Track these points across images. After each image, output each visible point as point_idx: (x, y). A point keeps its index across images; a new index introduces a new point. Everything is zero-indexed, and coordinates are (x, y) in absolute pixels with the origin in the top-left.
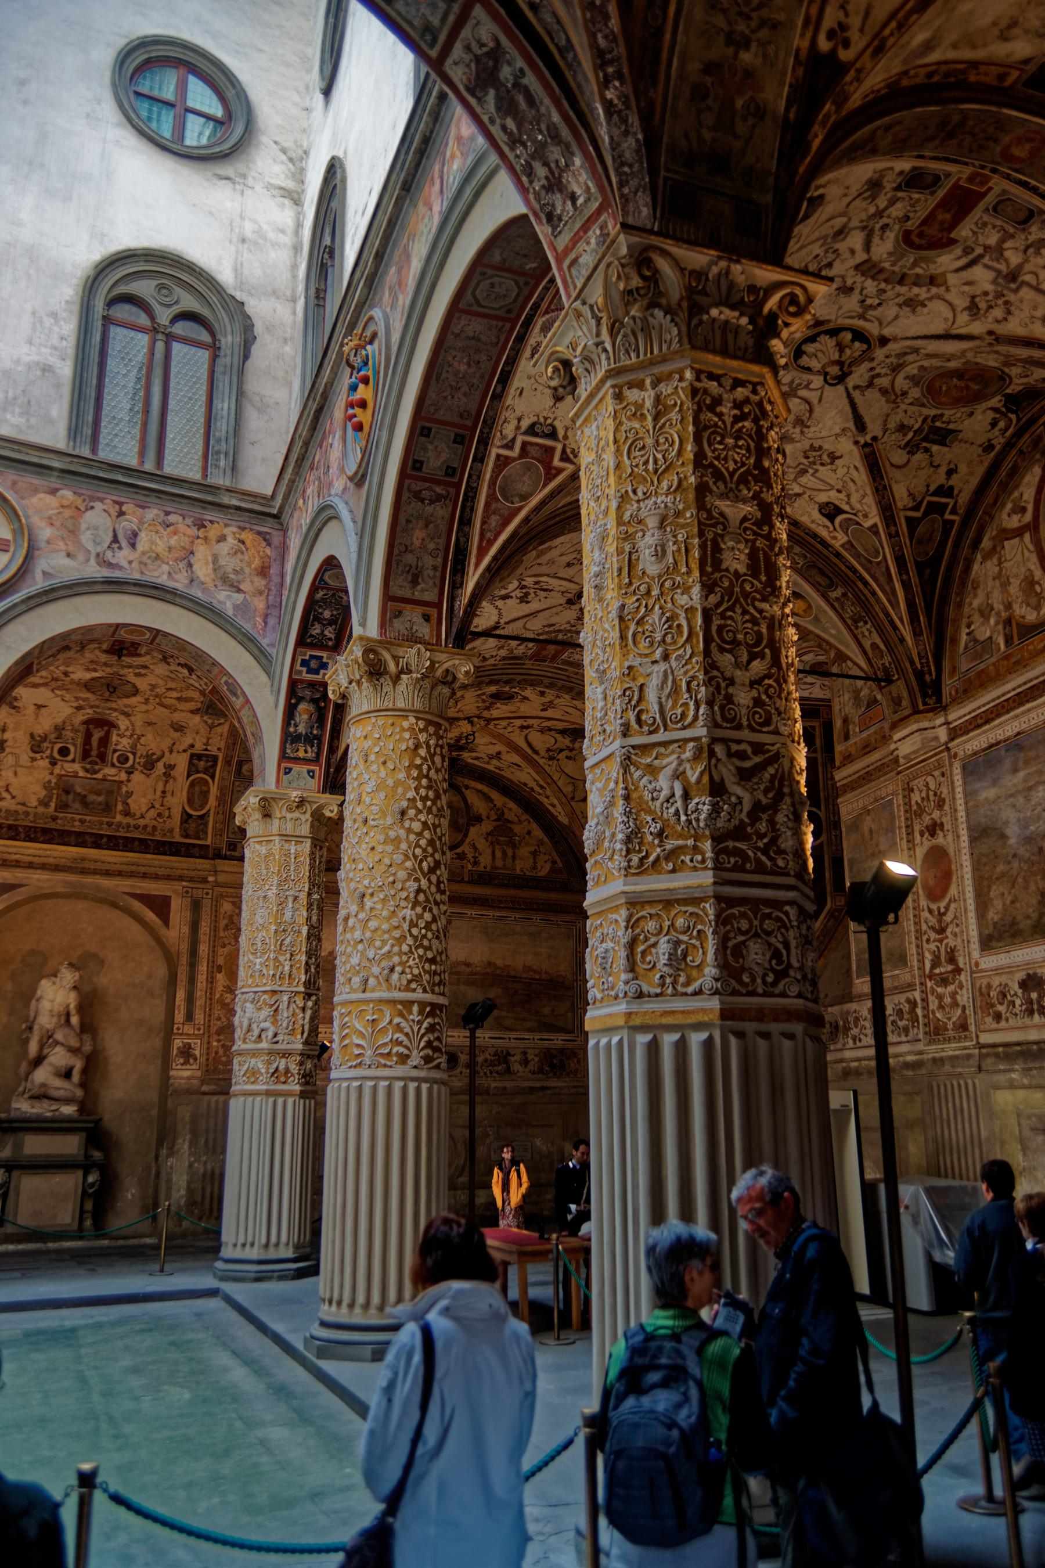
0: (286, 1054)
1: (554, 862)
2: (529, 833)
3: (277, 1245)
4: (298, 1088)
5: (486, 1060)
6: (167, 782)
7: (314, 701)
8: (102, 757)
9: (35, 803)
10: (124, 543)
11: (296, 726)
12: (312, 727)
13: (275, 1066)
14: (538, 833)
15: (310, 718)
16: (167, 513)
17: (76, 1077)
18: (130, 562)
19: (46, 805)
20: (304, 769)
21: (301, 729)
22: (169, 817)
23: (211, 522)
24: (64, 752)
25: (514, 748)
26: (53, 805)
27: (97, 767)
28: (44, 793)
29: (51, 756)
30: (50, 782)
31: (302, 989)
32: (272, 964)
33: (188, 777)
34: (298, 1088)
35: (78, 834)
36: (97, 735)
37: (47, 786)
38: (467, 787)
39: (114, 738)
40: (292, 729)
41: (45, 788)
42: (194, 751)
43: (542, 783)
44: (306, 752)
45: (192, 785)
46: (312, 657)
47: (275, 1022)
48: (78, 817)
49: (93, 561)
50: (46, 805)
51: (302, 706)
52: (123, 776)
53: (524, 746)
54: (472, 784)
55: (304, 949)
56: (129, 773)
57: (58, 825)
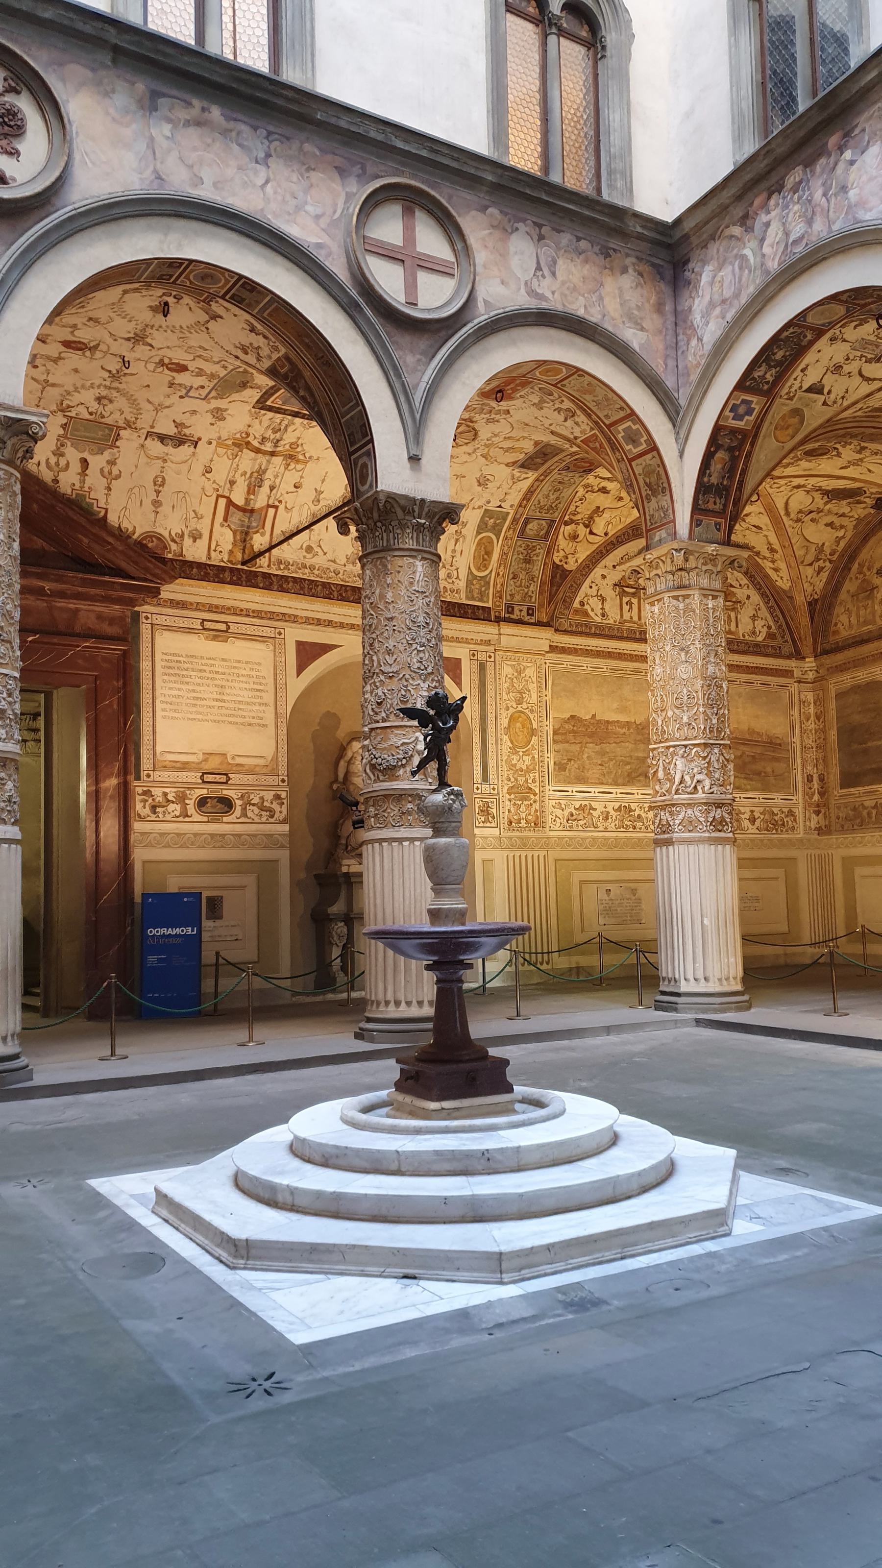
1: (769, 627)
2: (748, 597)
6: (457, 540)
7: (730, 449)
10: (546, 271)
12: (723, 478)
13: (712, 815)
14: (756, 598)
15: (723, 468)
16: (579, 239)
18: (553, 293)
21: (714, 480)
22: (457, 578)
23: (614, 250)
32: (702, 716)
33: (478, 533)
40: (706, 479)
42: (490, 507)
43: (777, 546)
44: (715, 503)
45: (479, 544)
46: (743, 401)
47: (709, 775)
49: (523, 291)
51: (720, 455)
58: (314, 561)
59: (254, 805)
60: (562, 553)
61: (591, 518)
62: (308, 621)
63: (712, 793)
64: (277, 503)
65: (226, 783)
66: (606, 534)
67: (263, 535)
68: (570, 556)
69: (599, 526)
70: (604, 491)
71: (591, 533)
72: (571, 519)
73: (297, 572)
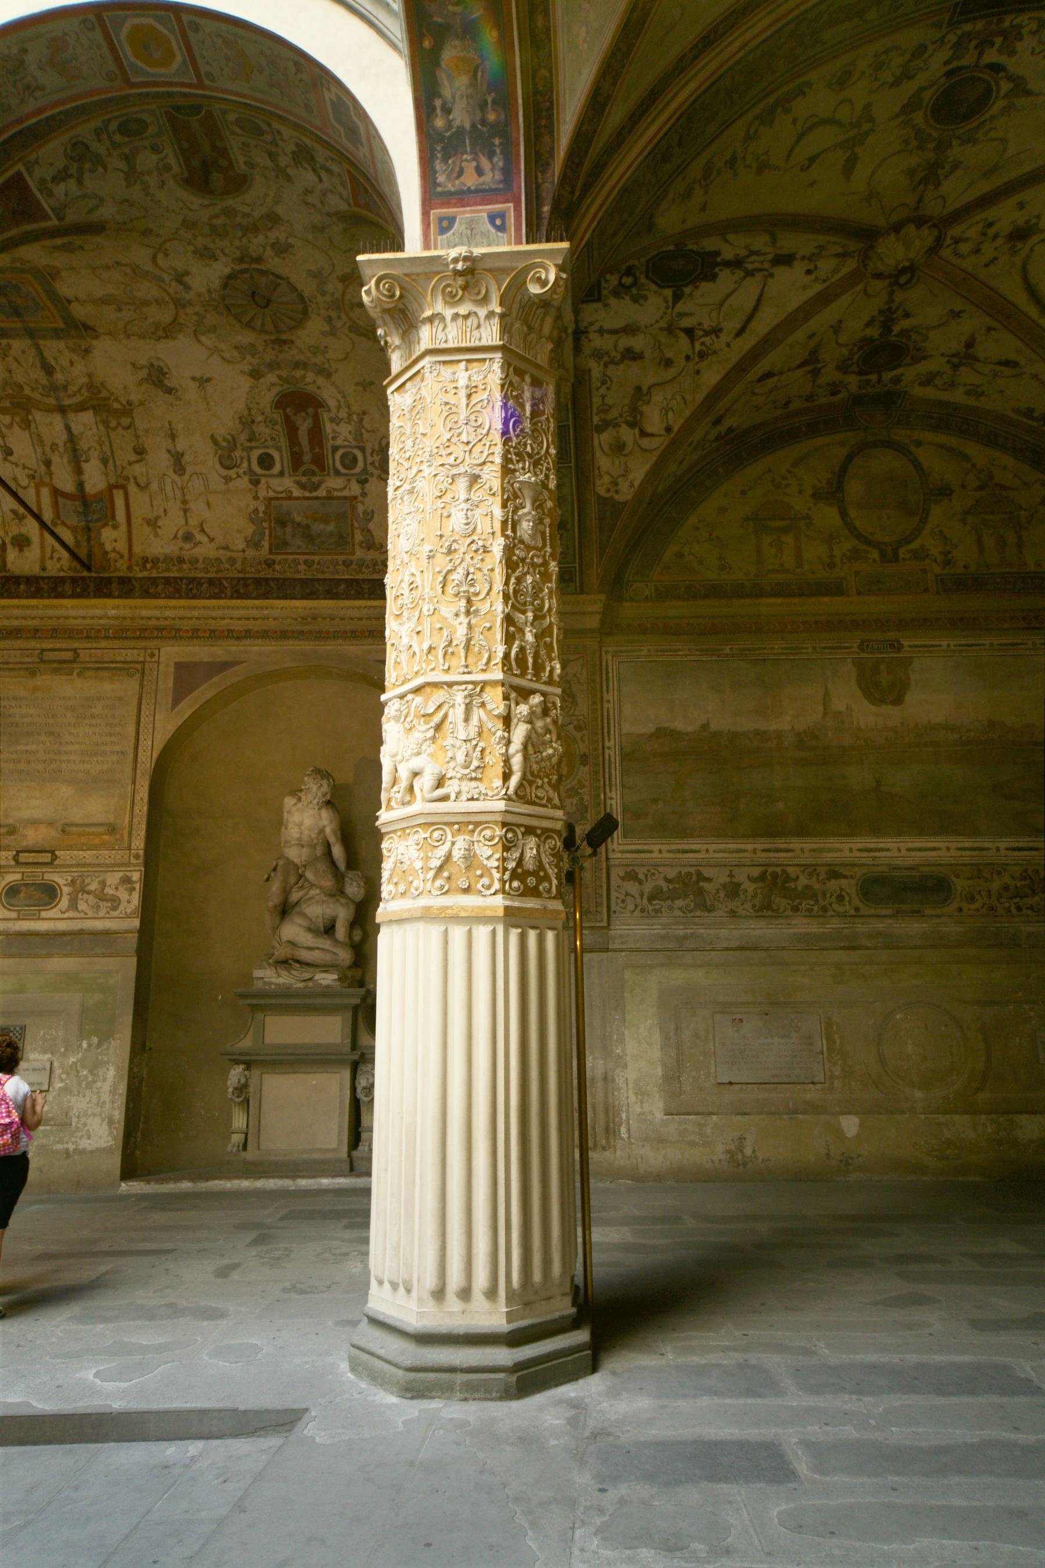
0: (468, 824)
3: (465, 1294)
4: (499, 902)
5: (1006, 888)
8: (319, 461)
9: (241, 545)
11: (447, 111)
17: (341, 932)
19: (257, 546)
20: (481, 213)
24: (266, 461)
25: (1001, 312)
26: (266, 544)
27: (315, 479)
28: (250, 529)
29: (250, 471)
30: (256, 511)
31: (498, 675)
34: (499, 902)
35: (304, 582)
36: (304, 426)
37: (253, 518)
38: (918, 444)
39: (329, 428)
40: (439, 123)
41: (252, 521)
44: (480, 172)
48: (302, 558)
50: (257, 546)
52: (355, 489)
53: (1020, 298)
54: (928, 436)
55: (498, 585)
56: (363, 482)
57: (278, 571)
58: (197, 551)
59: (88, 893)
60: (606, 479)
61: (634, 410)
62: (195, 634)
63: (445, 798)
64: (121, 481)
65: (51, 863)
66: (668, 429)
67: (115, 527)
68: (620, 480)
69: (654, 422)
70: (631, 355)
71: (644, 434)
72: (604, 421)
73: (169, 571)
